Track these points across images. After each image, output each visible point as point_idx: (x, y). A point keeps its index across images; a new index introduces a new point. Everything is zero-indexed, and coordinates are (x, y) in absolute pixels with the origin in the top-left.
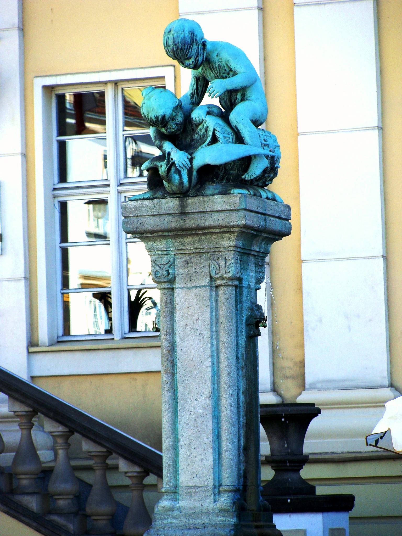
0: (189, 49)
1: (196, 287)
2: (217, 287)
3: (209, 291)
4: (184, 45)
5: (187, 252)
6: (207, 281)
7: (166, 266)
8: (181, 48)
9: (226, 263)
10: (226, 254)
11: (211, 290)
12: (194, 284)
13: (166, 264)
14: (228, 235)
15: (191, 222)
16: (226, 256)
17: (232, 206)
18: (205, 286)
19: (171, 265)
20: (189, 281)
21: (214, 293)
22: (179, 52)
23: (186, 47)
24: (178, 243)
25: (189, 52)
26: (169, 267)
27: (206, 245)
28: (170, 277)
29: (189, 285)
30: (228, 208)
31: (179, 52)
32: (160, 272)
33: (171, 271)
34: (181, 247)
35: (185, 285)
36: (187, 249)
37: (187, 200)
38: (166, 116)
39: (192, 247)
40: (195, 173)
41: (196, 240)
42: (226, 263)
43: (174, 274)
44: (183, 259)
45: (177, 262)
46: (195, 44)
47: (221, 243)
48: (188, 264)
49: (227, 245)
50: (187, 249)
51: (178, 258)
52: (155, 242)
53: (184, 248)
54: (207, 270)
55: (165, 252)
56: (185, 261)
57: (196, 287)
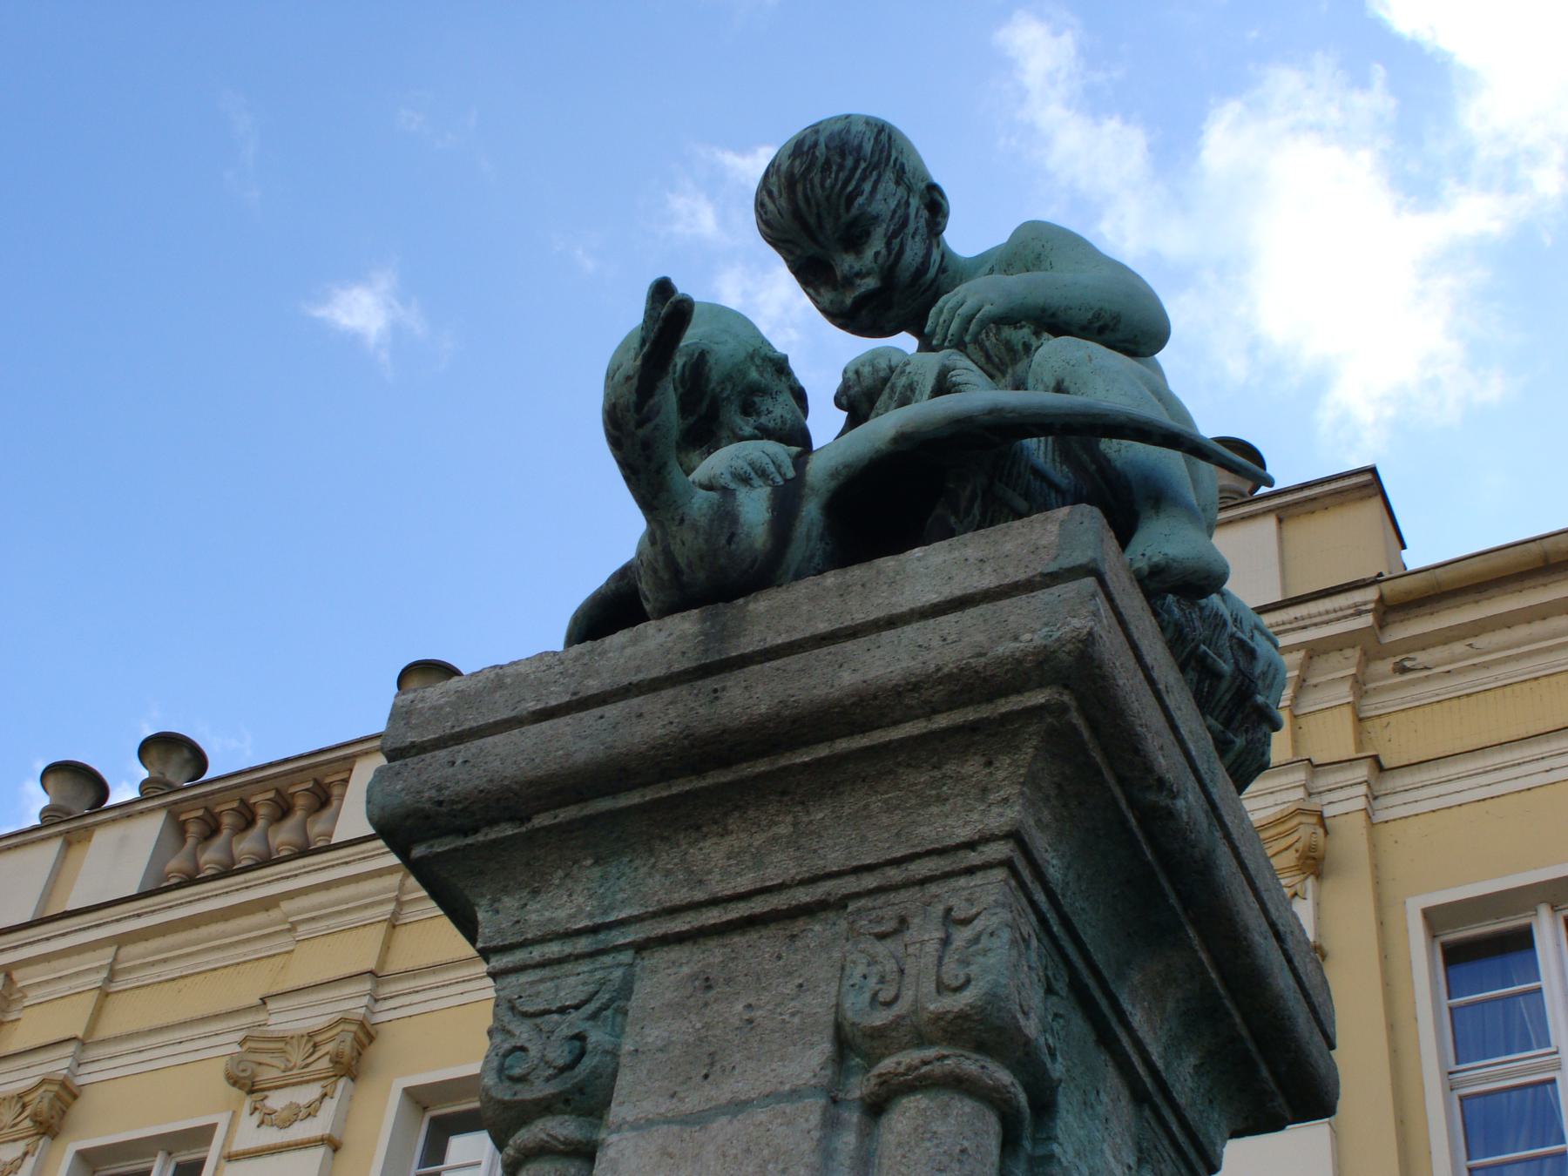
0: (863, 179)
1: (738, 1106)
2: (876, 1108)
3: (815, 1119)
4: (843, 155)
5: (713, 917)
6: (810, 1061)
7: (574, 1015)
8: (828, 162)
9: (946, 942)
10: (955, 894)
11: (831, 1123)
12: (726, 1090)
13: (577, 1007)
14: (972, 767)
15: (750, 697)
16: (953, 902)
17: (1010, 570)
18: (795, 1094)
19: (605, 1007)
20: (699, 1079)
21: (848, 1140)
22: (817, 181)
23: (849, 162)
24: (668, 873)
25: (858, 192)
26: (594, 1016)
27: (834, 859)
28: (588, 1063)
29: (693, 1101)
30: (988, 581)
31: (817, 181)
32: (534, 1051)
33: (596, 1036)
34: (681, 896)
35: (666, 1106)
36: (714, 902)
37: (746, 604)
38: (711, 360)
39: (744, 883)
40: (811, 510)
41: (775, 839)
42: (946, 942)
43: (614, 1053)
44: (686, 970)
45: (642, 989)
46: (889, 175)
47: (921, 830)
48: (709, 988)
49: (964, 834)
50: (714, 902)
51: (654, 971)
52: (535, 892)
53: (700, 895)
54: (819, 1005)
55: (583, 944)
56: (694, 977)
57: (738, 1106)
